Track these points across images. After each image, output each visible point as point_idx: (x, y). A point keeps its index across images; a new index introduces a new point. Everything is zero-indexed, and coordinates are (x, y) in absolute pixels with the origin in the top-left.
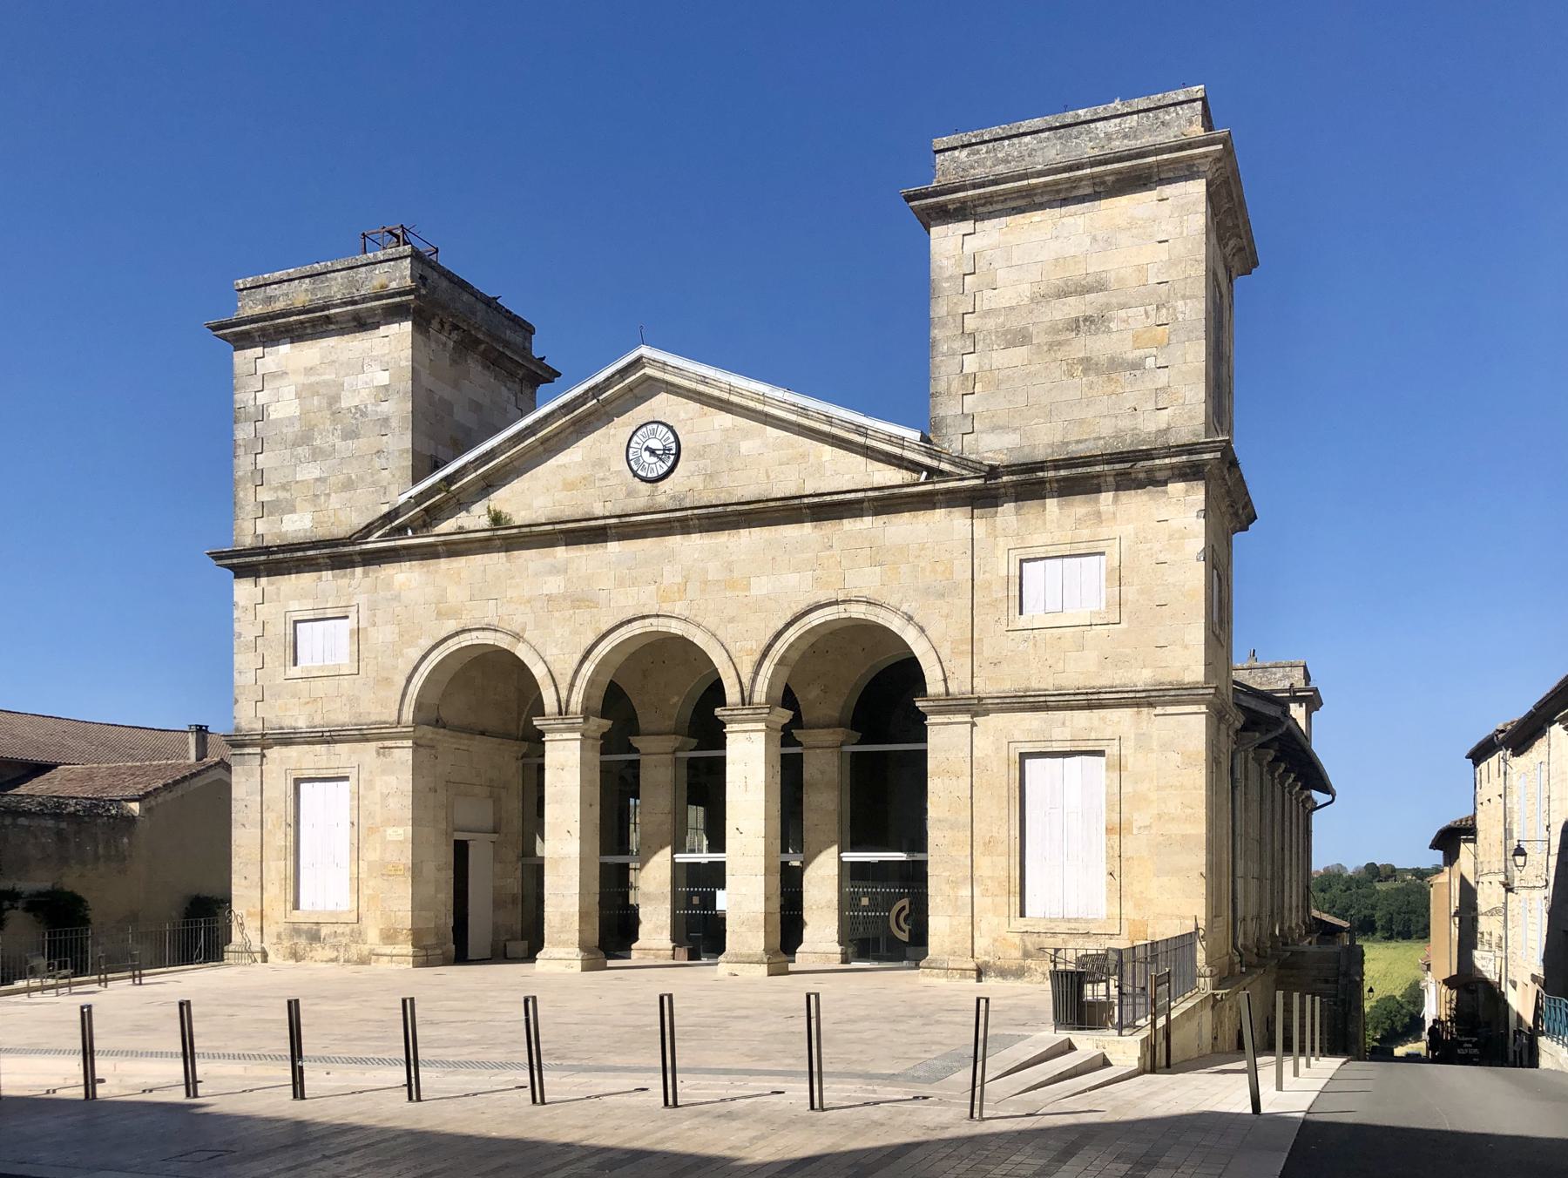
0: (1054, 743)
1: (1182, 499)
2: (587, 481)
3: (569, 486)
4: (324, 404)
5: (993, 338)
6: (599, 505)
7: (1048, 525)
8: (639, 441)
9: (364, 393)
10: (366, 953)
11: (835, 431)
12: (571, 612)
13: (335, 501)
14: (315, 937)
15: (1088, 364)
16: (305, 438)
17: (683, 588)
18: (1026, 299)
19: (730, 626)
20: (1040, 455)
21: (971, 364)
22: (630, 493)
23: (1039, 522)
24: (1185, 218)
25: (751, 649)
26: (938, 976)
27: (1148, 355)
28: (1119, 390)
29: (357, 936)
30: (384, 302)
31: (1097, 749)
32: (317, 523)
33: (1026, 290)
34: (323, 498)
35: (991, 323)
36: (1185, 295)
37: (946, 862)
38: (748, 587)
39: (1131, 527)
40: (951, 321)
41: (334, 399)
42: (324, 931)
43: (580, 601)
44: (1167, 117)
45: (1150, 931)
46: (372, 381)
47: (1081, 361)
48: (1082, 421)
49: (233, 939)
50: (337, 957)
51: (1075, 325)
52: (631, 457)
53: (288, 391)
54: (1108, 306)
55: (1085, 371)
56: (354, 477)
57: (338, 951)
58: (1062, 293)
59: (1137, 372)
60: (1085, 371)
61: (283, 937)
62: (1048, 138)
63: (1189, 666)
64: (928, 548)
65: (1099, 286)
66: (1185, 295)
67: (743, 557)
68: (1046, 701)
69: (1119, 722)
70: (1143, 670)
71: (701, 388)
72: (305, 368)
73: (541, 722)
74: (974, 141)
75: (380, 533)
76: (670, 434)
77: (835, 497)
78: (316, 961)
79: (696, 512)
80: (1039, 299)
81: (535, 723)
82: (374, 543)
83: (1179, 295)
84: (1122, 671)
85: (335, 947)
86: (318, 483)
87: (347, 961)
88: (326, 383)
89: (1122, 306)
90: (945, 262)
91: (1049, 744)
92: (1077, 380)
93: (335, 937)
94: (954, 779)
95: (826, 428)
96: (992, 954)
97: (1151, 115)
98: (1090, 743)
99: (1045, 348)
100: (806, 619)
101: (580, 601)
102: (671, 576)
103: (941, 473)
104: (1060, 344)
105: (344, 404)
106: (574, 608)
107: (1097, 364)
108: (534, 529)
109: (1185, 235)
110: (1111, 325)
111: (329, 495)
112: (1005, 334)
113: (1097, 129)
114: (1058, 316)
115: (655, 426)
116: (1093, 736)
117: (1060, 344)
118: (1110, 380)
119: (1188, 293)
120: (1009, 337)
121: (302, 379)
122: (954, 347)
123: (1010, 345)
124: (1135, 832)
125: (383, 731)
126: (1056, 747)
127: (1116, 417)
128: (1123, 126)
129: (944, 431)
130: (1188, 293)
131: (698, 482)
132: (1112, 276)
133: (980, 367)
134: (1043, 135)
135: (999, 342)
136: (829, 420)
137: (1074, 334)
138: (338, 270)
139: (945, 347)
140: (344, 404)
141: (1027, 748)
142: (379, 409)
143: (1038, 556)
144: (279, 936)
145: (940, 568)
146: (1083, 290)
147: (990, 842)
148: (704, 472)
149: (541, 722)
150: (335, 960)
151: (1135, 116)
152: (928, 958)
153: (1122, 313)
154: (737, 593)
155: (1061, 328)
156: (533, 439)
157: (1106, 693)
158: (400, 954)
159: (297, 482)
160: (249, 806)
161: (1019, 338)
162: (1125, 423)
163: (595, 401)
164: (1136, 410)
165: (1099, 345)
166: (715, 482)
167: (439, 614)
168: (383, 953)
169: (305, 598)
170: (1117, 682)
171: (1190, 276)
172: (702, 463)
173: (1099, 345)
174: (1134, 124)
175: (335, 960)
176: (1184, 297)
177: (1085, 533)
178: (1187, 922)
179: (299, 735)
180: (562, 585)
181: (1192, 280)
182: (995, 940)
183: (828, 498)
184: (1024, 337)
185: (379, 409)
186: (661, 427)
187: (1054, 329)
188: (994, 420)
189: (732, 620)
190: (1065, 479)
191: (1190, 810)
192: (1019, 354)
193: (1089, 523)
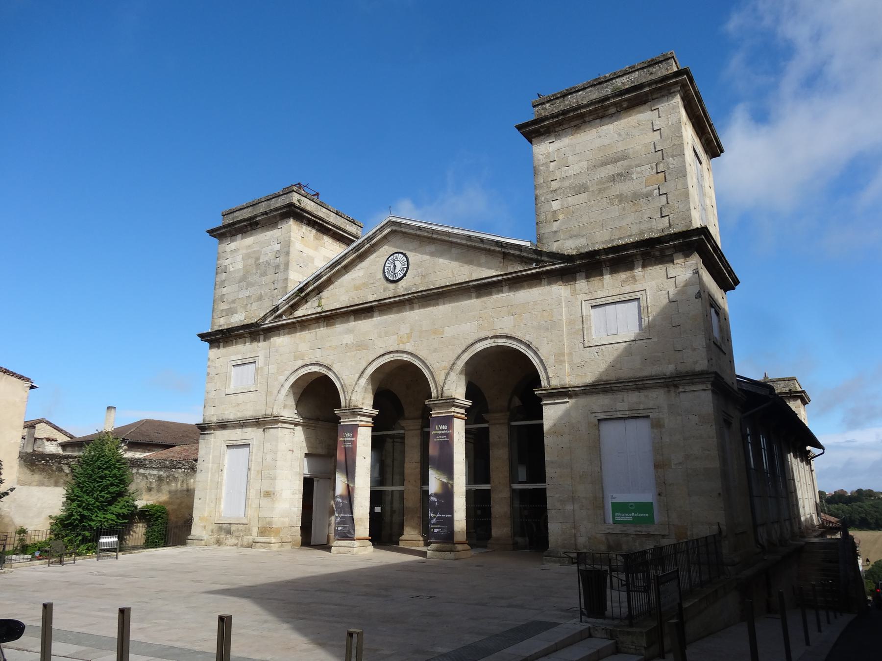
0: (618, 412)
1: (683, 264)
2: (365, 285)
3: (357, 288)
4: (253, 262)
5: (568, 191)
6: (370, 297)
7: (605, 286)
8: (390, 263)
9: (270, 255)
10: (251, 541)
11: (486, 246)
12: (355, 352)
13: (255, 305)
14: (229, 532)
15: (621, 198)
16: (243, 279)
17: (409, 336)
18: (584, 169)
19: (434, 354)
20: (598, 247)
21: (555, 205)
22: (385, 289)
23: (600, 284)
24: (669, 116)
25: (445, 367)
26: (555, 562)
27: (654, 189)
28: (640, 209)
29: (248, 532)
30: (280, 212)
31: (645, 415)
32: (246, 317)
33: (584, 164)
34: (249, 305)
35: (567, 183)
36: (673, 155)
37: (557, 488)
38: (443, 333)
39: (654, 283)
40: (545, 185)
41: (257, 259)
42: (233, 528)
43: (360, 346)
44: (654, 70)
45: (689, 533)
46: (273, 249)
47: (617, 196)
48: (620, 228)
49: (192, 532)
50: (237, 543)
51: (613, 179)
52: (386, 271)
53: (239, 258)
54: (630, 167)
55: (620, 201)
56: (263, 294)
57: (238, 539)
58: (604, 164)
59: (650, 198)
60: (620, 201)
61: (214, 531)
62: (591, 91)
63: (697, 361)
64: (539, 304)
65: (624, 157)
66: (673, 155)
67: (440, 317)
68: (611, 387)
69: (657, 398)
70: (669, 365)
71: (419, 233)
72: (247, 246)
73: (338, 412)
74: (552, 98)
75: (270, 319)
76: (404, 258)
77: (487, 280)
78: (227, 545)
79: (415, 295)
80: (594, 167)
81: (335, 412)
82: (268, 324)
83: (669, 155)
84: (656, 366)
85: (237, 538)
86: (248, 298)
87: (242, 546)
88: (254, 252)
89: (638, 166)
90: (541, 157)
91: (615, 413)
92: (616, 206)
93: (238, 532)
94: (559, 436)
95: (481, 245)
96: (588, 548)
97: (645, 70)
98: (640, 412)
99: (597, 192)
100: (473, 348)
101: (360, 346)
102: (404, 329)
103: (543, 261)
104: (605, 189)
105: (261, 261)
106: (356, 350)
107: (626, 197)
108: (338, 311)
109: (670, 124)
110: (632, 176)
111: (252, 303)
112: (574, 188)
113: (616, 82)
114: (603, 175)
115: (397, 254)
116: (642, 406)
117: (605, 189)
118: (634, 204)
119: (674, 154)
120: (576, 189)
121: (245, 251)
122: (548, 197)
123: (578, 193)
124: (673, 467)
125: (266, 419)
126: (620, 415)
127: (640, 223)
128: (630, 78)
129: (545, 241)
130: (674, 154)
131: (418, 280)
132: (631, 152)
133: (562, 206)
134: (588, 90)
135: (571, 192)
136: (482, 240)
137: (612, 183)
138: (263, 201)
139: (543, 198)
140: (261, 261)
141: (602, 416)
142: (276, 261)
143: (601, 303)
144: (212, 531)
145: (545, 314)
146: (615, 161)
147: (583, 475)
148: (421, 275)
149: (338, 412)
150: (236, 545)
151: (637, 73)
152: (548, 550)
153: (638, 169)
154: (437, 336)
155: (604, 181)
156: (340, 266)
157: (647, 380)
158: (266, 542)
159: (239, 299)
160: (205, 461)
161: (582, 189)
162: (645, 226)
163: (368, 245)
164: (651, 218)
165: (626, 188)
166: (427, 279)
167: (295, 357)
168: (258, 541)
169: (238, 354)
170: (654, 373)
171: (675, 145)
172: (419, 270)
173: (626, 188)
174: (636, 76)
175: (236, 545)
176: (673, 156)
177: (627, 289)
178: (714, 527)
179: (228, 423)
180: (352, 338)
181: (676, 146)
182: (590, 538)
183: (483, 281)
184: (585, 188)
185: (276, 261)
186: (400, 255)
187: (600, 182)
188: (571, 232)
189: (435, 351)
190: (612, 259)
191: (707, 452)
192: (583, 197)
193: (629, 282)
